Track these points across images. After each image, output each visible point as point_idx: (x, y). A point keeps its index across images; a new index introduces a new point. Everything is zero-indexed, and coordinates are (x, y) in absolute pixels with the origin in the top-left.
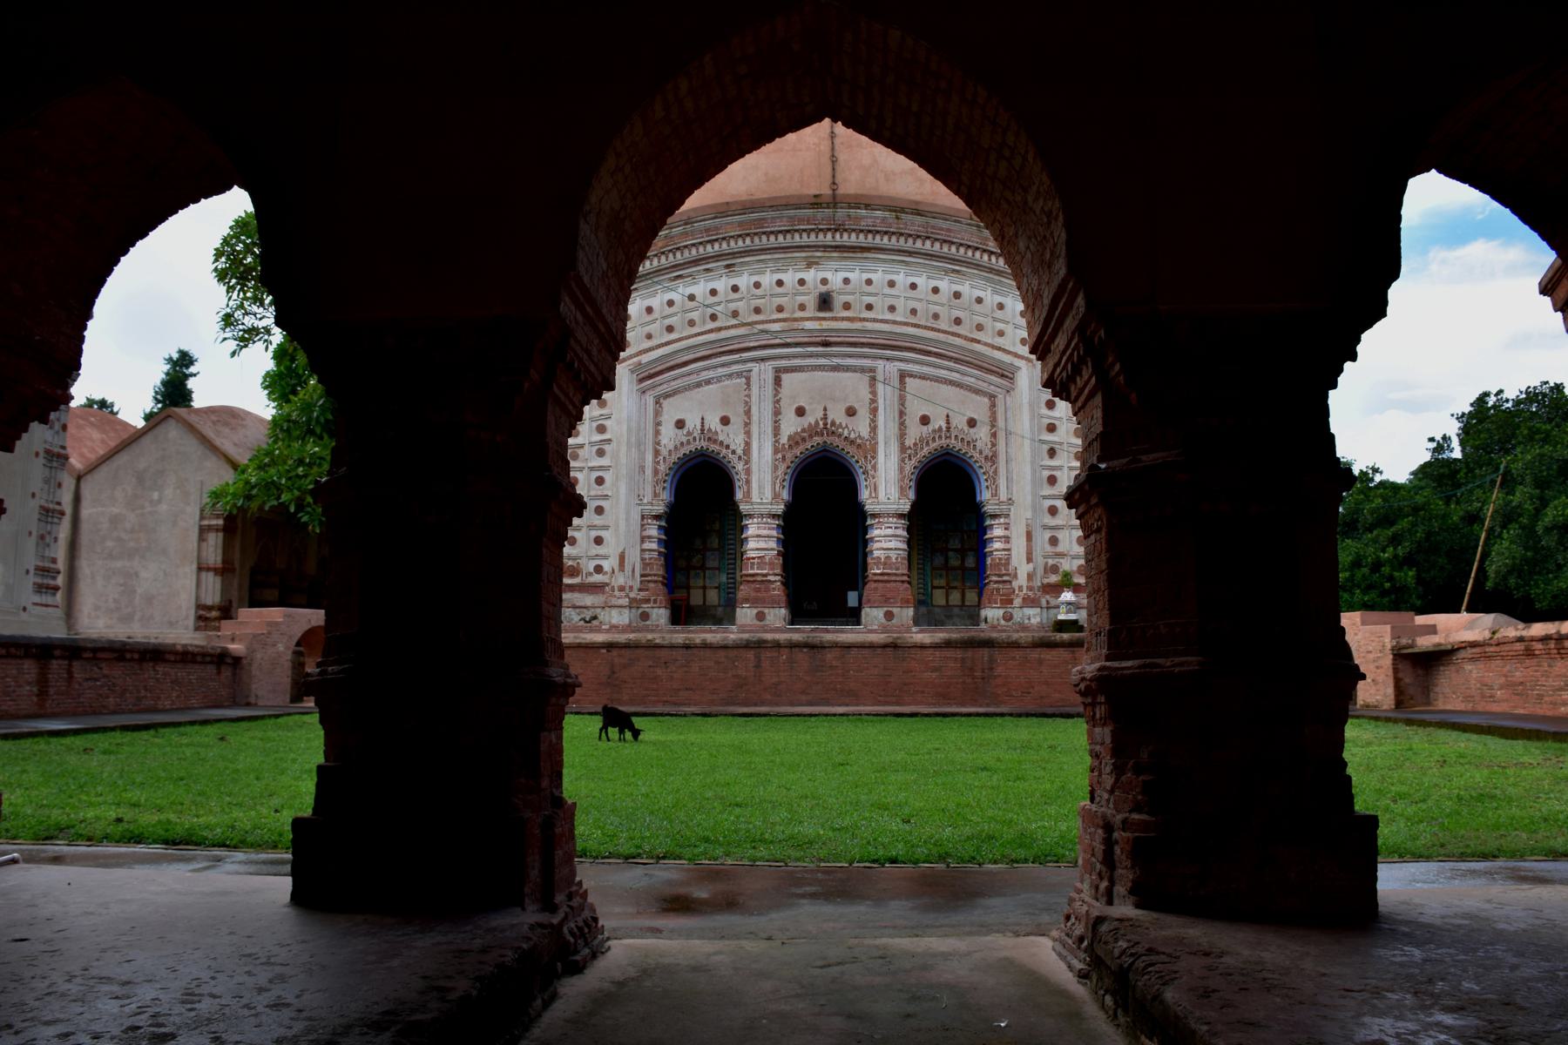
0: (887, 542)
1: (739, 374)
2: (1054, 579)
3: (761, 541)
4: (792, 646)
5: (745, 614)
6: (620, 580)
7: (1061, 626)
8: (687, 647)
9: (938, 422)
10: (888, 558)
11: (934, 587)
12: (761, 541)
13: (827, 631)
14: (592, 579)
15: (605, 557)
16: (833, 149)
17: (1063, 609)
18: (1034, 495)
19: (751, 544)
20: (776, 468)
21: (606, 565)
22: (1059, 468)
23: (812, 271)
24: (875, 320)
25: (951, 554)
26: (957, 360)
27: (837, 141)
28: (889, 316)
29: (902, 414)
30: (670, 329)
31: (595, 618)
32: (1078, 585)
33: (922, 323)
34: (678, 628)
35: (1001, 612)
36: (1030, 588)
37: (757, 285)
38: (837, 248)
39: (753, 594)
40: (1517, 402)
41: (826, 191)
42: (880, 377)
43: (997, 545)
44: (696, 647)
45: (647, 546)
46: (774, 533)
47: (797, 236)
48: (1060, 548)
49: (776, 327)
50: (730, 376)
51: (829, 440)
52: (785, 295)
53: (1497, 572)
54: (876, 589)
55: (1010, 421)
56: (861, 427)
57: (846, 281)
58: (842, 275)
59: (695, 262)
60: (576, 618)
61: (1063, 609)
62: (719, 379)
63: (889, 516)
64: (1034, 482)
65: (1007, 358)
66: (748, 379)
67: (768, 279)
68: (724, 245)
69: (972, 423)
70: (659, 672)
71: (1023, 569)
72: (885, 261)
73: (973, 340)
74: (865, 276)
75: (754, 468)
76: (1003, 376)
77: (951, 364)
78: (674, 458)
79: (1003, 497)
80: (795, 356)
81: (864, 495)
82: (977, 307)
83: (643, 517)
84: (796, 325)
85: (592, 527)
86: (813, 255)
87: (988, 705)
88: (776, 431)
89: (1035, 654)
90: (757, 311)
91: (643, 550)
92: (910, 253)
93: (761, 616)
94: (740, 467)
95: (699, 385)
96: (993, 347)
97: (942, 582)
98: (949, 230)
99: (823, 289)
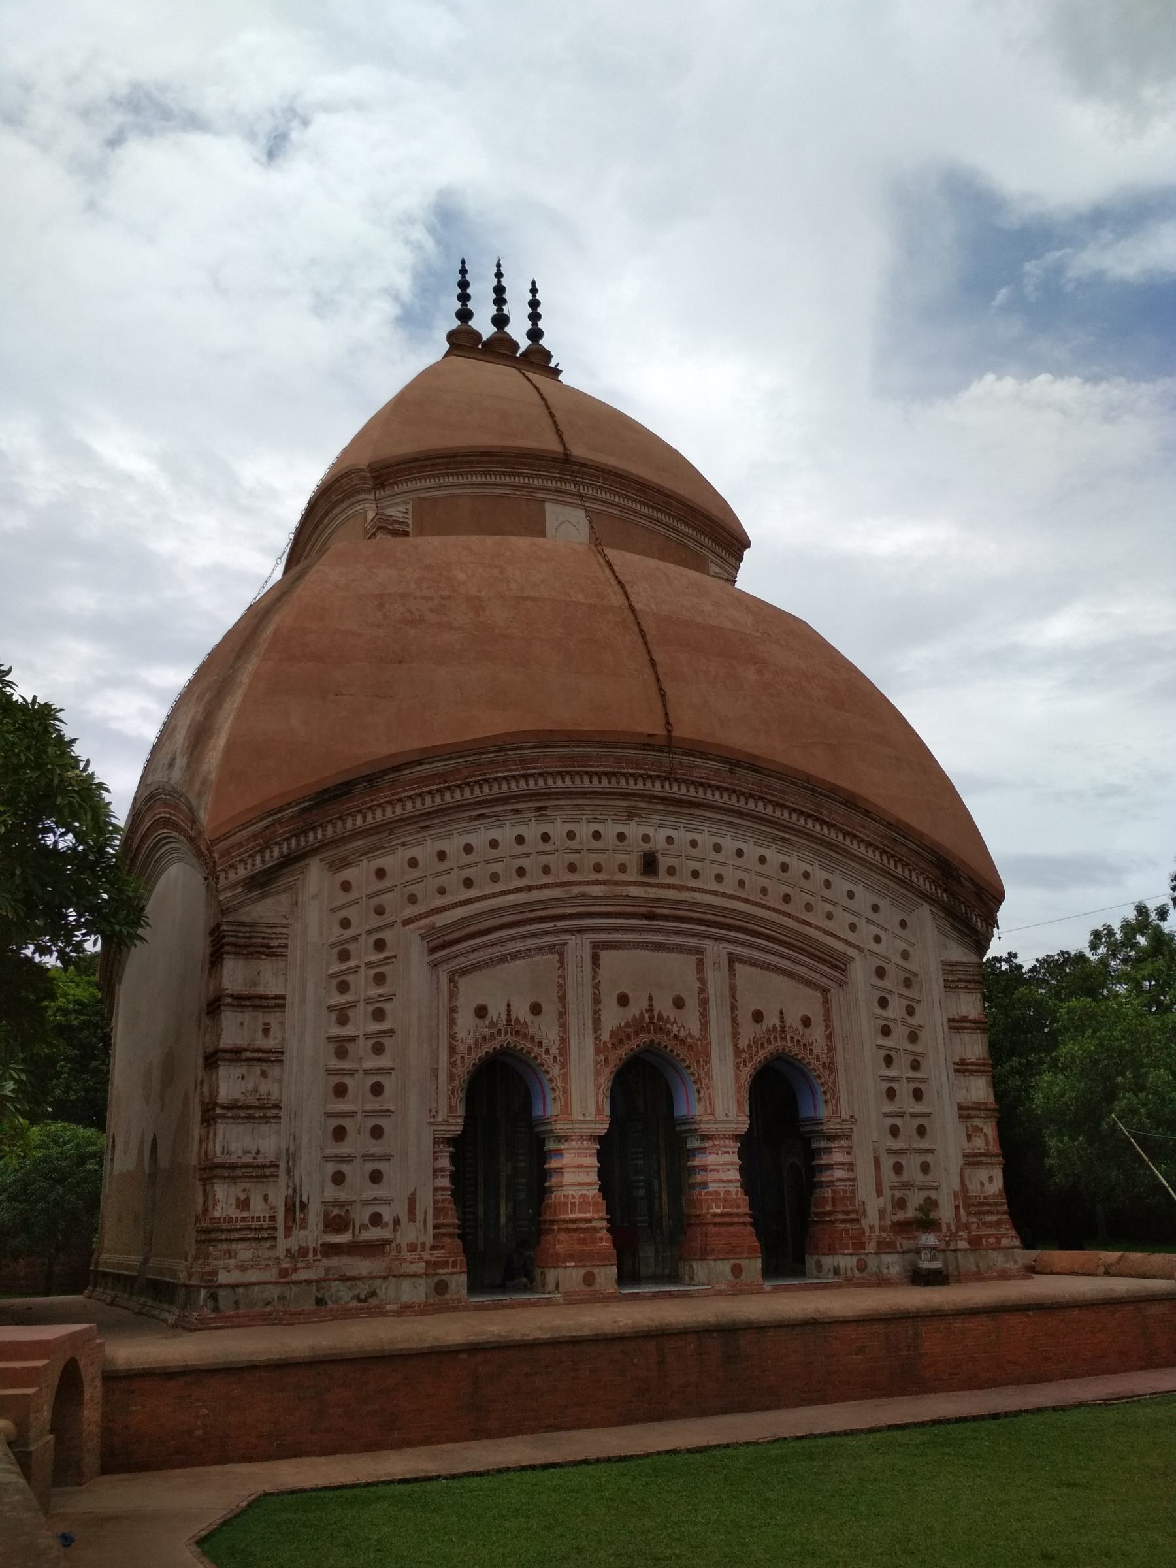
6: (410, 1234)
9: (772, 1020)
15: (387, 1202)
19: (568, 1177)
20: (598, 1074)
21: (387, 1215)
24: (704, 891)
27: (660, 670)
29: (733, 1008)
30: (468, 883)
33: (772, 904)
35: (854, 1259)
36: (883, 1229)
38: (664, 800)
39: (577, 1247)
41: (661, 731)
42: (709, 962)
43: (839, 1174)
48: (905, 1177)
49: (597, 890)
50: (540, 950)
51: (660, 1038)
52: (603, 851)
54: (718, 1235)
56: (690, 1022)
57: (670, 840)
58: (663, 833)
62: (527, 954)
63: (725, 1137)
65: (840, 946)
66: (561, 954)
67: (584, 830)
68: (541, 783)
69: (806, 1022)
72: (711, 820)
76: (835, 967)
78: (475, 1057)
80: (616, 929)
83: (436, 1142)
84: (620, 890)
85: (367, 1157)
88: (597, 1021)
90: (572, 868)
91: (436, 1190)
92: (740, 814)
93: (589, 1279)
94: (555, 1071)
95: (503, 959)
98: (782, 792)
99: (647, 847)
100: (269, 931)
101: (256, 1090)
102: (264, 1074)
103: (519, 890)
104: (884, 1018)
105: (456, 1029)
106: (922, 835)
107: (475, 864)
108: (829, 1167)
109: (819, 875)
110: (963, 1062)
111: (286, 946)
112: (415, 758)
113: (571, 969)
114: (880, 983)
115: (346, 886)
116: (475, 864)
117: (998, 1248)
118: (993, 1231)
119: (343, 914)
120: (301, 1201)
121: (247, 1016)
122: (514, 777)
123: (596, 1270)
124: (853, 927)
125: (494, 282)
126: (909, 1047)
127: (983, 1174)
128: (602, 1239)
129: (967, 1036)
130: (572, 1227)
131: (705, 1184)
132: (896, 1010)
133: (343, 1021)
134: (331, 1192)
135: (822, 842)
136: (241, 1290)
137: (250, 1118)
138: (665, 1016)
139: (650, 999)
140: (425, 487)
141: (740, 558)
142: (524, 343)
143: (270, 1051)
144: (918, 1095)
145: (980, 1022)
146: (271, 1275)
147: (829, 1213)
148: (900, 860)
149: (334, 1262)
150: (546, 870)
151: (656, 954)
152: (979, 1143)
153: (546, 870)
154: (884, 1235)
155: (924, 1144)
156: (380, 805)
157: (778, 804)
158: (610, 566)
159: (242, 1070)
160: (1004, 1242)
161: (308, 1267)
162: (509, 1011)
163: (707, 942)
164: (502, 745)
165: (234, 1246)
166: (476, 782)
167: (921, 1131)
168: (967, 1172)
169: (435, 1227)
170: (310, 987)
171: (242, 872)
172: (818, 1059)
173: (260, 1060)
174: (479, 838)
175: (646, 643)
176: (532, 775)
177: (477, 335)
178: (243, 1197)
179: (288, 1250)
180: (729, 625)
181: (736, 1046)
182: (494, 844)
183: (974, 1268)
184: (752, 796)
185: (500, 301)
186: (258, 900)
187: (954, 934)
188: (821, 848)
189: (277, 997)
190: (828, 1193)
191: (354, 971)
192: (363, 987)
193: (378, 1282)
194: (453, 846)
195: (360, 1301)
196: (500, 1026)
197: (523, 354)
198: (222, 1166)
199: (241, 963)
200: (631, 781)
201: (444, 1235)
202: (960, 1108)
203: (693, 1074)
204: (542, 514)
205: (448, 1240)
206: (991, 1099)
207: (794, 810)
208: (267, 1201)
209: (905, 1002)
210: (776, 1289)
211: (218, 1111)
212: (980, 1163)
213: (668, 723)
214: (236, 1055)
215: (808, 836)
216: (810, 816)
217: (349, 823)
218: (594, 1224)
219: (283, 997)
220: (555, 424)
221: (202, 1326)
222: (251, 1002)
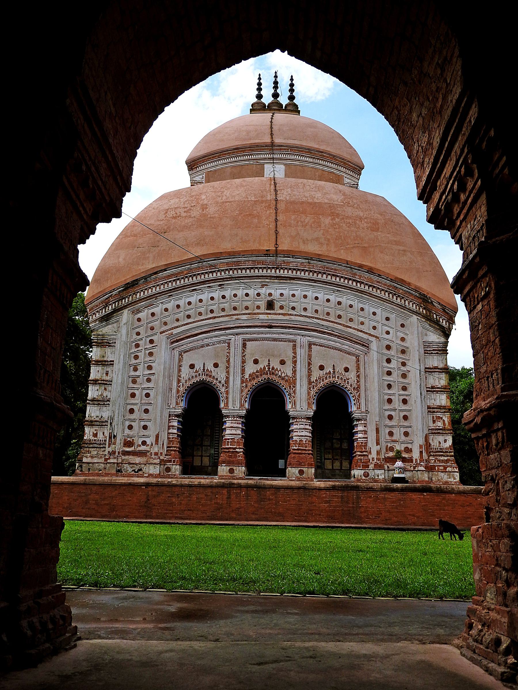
0: (301, 433)
1: (224, 342)
2: (391, 454)
3: (233, 431)
4: (248, 487)
5: (223, 470)
6: (156, 449)
7: (396, 480)
8: (190, 486)
11: (325, 459)
12: (233, 431)
13: (267, 480)
14: (140, 448)
15: (148, 437)
16: (276, 227)
17: (397, 471)
18: (380, 409)
19: (228, 432)
20: (242, 391)
21: (149, 441)
22: (394, 394)
25: (334, 441)
26: (339, 337)
27: (279, 223)
28: (303, 313)
29: (309, 364)
30: (189, 317)
32: (405, 458)
34: (186, 476)
35: (363, 472)
42: (298, 345)
43: (360, 435)
45: (171, 431)
46: (240, 426)
49: (244, 317)
50: (219, 342)
54: (294, 458)
55: (367, 369)
56: (288, 370)
59: (204, 283)
60: (130, 470)
61: (397, 471)
64: (379, 402)
65: (365, 336)
66: (229, 344)
67: (240, 293)
68: (219, 274)
69: (347, 370)
70: (174, 500)
71: (374, 449)
73: (347, 327)
74: (292, 292)
75: (231, 391)
76: (363, 345)
78: (188, 384)
79: (363, 409)
81: (289, 406)
83: (169, 417)
85: (141, 420)
87: (356, 523)
88: (243, 371)
90: (235, 309)
92: (315, 281)
93: (231, 471)
94: (223, 390)
95: (202, 346)
96: (358, 330)
97: (330, 456)
98: (335, 270)
99: (269, 299)
100: (109, 337)
102: (105, 389)
104: (388, 368)
105: (181, 373)
106: (409, 284)
107: (192, 309)
108: (357, 432)
109: (357, 305)
110: (433, 387)
111: (115, 343)
114: (387, 352)
115: (139, 320)
116: (192, 309)
117: (444, 471)
118: (443, 464)
119: (137, 330)
120: (114, 435)
121: (100, 368)
122: (206, 273)
123: (235, 468)
124: (374, 328)
127: (441, 438)
128: (239, 456)
129: (436, 375)
133: (136, 370)
135: (357, 291)
136: (91, 465)
137: (99, 404)
138: (275, 368)
139: (269, 361)
140: (210, 166)
141: (360, 174)
143: (107, 381)
144: (405, 402)
145: (444, 369)
148: (399, 296)
149: (126, 457)
151: (273, 342)
152: (440, 424)
153: (223, 310)
154: (378, 462)
156: (150, 288)
157: (333, 275)
159: (98, 388)
160: (449, 469)
161: (115, 458)
162: (204, 366)
163: (299, 337)
164: (200, 259)
165: (91, 449)
166: (190, 276)
168: (431, 437)
169: (167, 447)
172: (351, 386)
173: (103, 384)
176: (214, 271)
178: (95, 432)
179: (109, 452)
180: (326, 201)
182: (201, 301)
183: (427, 479)
184: (320, 273)
187: (432, 329)
188: (357, 293)
189: (111, 361)
191: (140, 351)
195: (135, 472)
196: (200, 372)
197: (285, 107)
198: (87, 421)
200: (261, 270)
201: (171, 450)
203: (287, 392)
207: (342, 277)
211: (88, 402)
212: (439, 433)
213: (276, 244)
215: (350, 289)
216: (350, 279)
218: (237, 450)
219: (113, 361)
220: (272, 131)
221: (77, 475)
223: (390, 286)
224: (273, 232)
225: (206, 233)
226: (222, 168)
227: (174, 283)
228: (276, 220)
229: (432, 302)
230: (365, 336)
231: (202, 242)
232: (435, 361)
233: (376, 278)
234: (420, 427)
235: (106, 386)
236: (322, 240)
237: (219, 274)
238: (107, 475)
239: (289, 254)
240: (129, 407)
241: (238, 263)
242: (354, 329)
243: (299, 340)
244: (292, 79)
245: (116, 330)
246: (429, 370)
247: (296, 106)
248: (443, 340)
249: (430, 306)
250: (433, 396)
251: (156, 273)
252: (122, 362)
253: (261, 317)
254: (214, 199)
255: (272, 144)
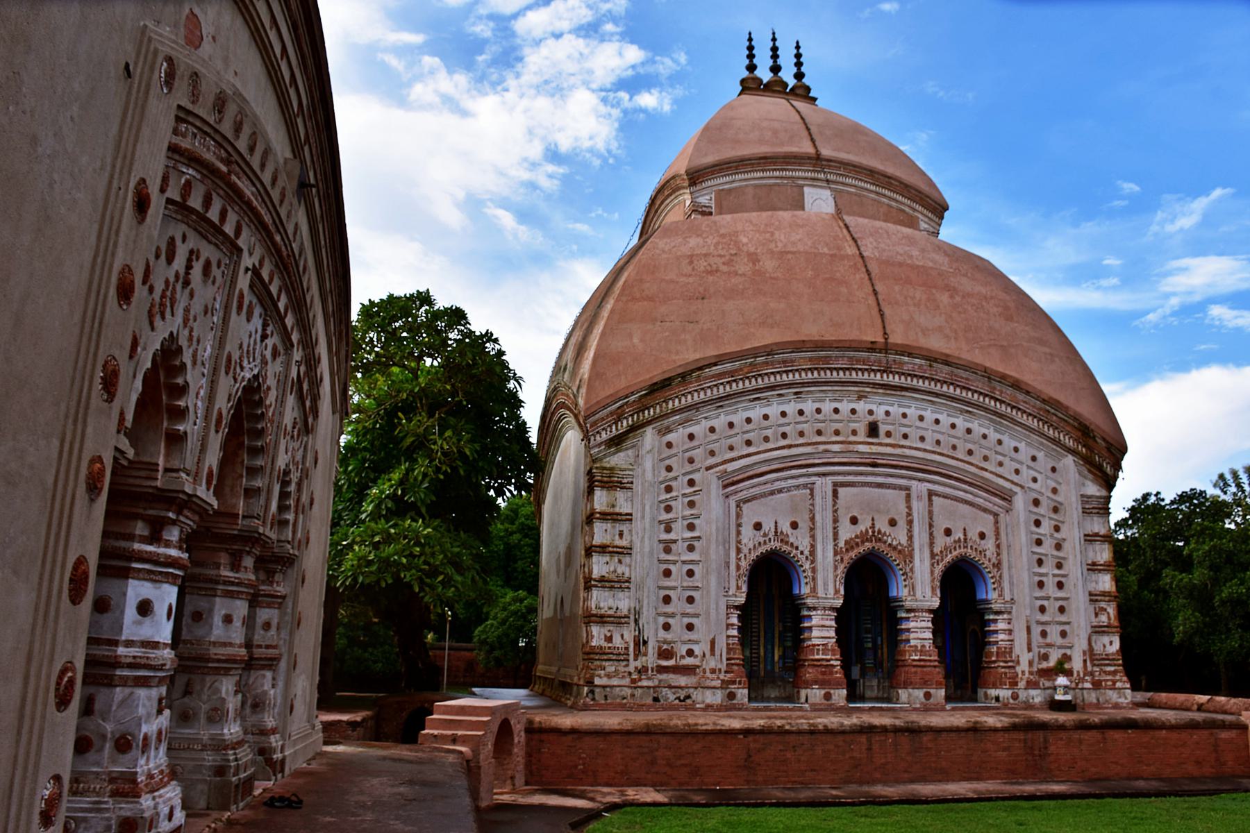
0: (919, 633)
3: (821, 630)
4: (896, 730)
6: (712, 663)
10: (923, 646)
15: (697, 642)
17: (1060, 691)
19: (815, 633)
20: (836, 568)
21: (697, 650)
22: (1046, 575)
23: (862, 402)
24: (910, 448)
26: (971, 484)
27: (880, 297)
28: (920, 445)
29: (931, 526)
30: (749, 443)
31: (688, 697)
35: (1010, 692)
36: (1031, 673)
37: (818, 411)
40: (1172, 502)
42: (914, 495)
43: (1001, 636)
44: (820, 732)
47: (854, 373)
48: (1048, 640)
49: (836, 448)
50: (798, 487)
51: (877, 545)
52: (841, 421)
53: (1185, 632)
56: (899, 535)
57: (887, 413)
58: (883, 408)
59: (772, 388)
60: (672, 697)
61: (1060, 691)
62: (789, 489)
63: (922, 611)
65: (1007, 485)
66: (812, 490)
67: (827, 407)
68: (797, 375)
69: (982, 536)
70: (789, 755)
71: (1025, 658)
74: (902, 410)
75: (819, 568)
76: (1004, 499)
77: (966, 487)
78: (753, 556)
80: (849, 474)
82: (983, 442)
84: (851, 447)
85: (684, 615)
86: (864, 390)
89: (1076, 735)
90: (819, 433)
91: (728, 637)
93: (828, 696)
94: (807, 566)
95: (772, 493)
99: (871, 418)
101: (615, 571)
102: (620, 562)
103: (783, 448)
106: (1067, 408)
107: (753, 430)
108: (996, 632)
109: (993, 436)
110: (1094, 564)
112: (713, 361)
113: (818, 500)
115: (669, 445)
116: (753, 430)
117: (1113, 688)
119: (668, 462)
121: (609, 525)
124: (1017, 472)
125: (771, 44)
126: (1056, 553)
127: (1105, 639)
129: (1097, 546)
130: (816, 664)
131: (908, 641)
132: (1046, 528)
133: (668, 530)
134: (662, 634)
135: (996, 413)
137: (612, 587)
141: (942, 218)
142: (792, 82)
144: (1060, 585)
146: (627, 681)
147: (994, 662)
149: (664, 676)
150: (801, 434)
152: (1103, 618)
153: (801, 434)
155: (1063, 618)
157: (964, 388)
158: (847, 227)
159: (607, 558)
160: (1119, 685)
161: (649, 679)
164: (770, 351)
167: (1062, 610)
168: (1094, 637)
170: (647, 508)
171: (604, 436)
174: (756, 413)
175: (870, 279)
177: (761, 81)
180: (931, 264)
181: (932, 551)
183: (1095, 701)
185: (775, 56)
186: (614, 453)
187: (1090, 476)
190: (994, 649)
191: (675, 499)
192: (679, 507)
193: (692, 690)
194: (738, 418)
197: (792, 90)
198: (595, 615)
199: (605, 492)
202: (1091, 594)
204: (803, 194)
205: (735, 668)
206: (1114, 589)
208: (623, 637)
209: (1053, 523)
210: (953, 709)
212: (1104, 632)
214: (603, 549)
215: (986, 410)
216: (986, 395)
217: (670, 405)
220: (810, 134)
221: (586, 708)
222: (611, 517)
223: (1040, 409)
224: (875, 312)
225: (772, 305)
226: (740, 187)
227: (728, 387)
228: (875, 293)
229: (1094, 437)
230: (1007, 485)
231: (770, 321)
232: (1096, 526)
233: (1021, 397)
234: (1083, 624)
235: (621, 557)
236: (947, 331)
237: (797, 375)
238: (640, 707)
239: (908, 351)
240: (663, 593)
241: (826, 359)
242: (991, 472)
243: (914, 489)
244: (798, 47)
245: (632, 460)
246: (1090, 538)
247: (808, 89)
248: (1104, 493)
249: (1090, 442)
250: (1094, 576)
251: (700, 369)
252: (648, 516)
253: (862, 448)
254: (764, 245)
255: (818, 157)
